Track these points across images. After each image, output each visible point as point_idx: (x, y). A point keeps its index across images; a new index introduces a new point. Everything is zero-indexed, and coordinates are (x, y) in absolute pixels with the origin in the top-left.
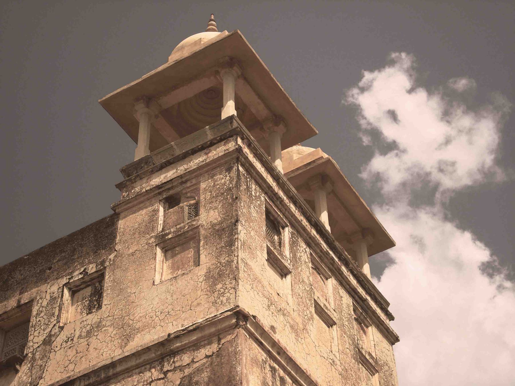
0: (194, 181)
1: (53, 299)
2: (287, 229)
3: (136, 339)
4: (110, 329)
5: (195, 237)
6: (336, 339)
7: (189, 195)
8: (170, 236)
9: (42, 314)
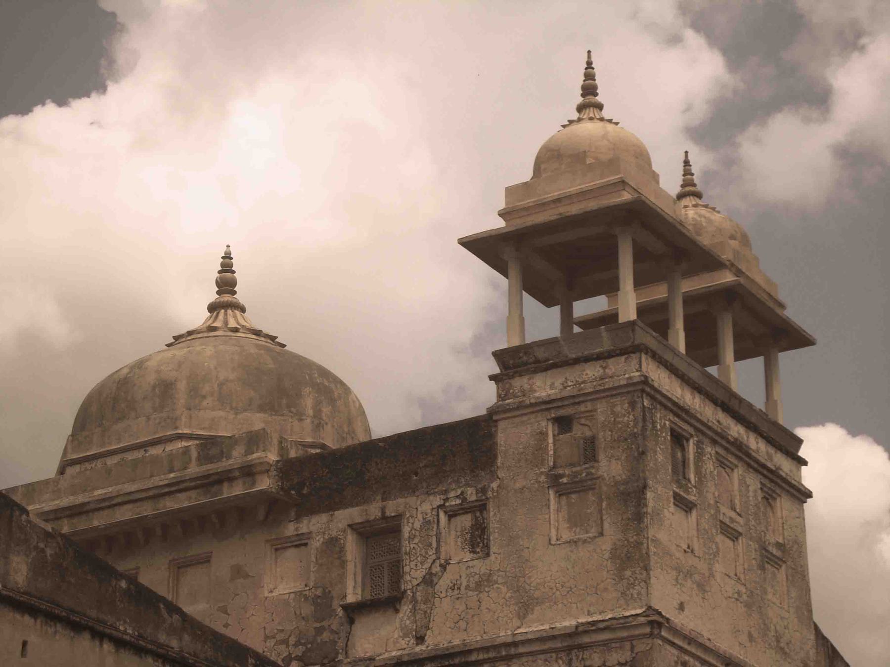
0: (589, 406)
1: (427, 523)
2: (691, 442)
3: (535, 611)
4: (504, 589)
5: (594, 489)
6: (741, 555)
7: (583, 421)
8: (565, 480)
9: (416, 541)
